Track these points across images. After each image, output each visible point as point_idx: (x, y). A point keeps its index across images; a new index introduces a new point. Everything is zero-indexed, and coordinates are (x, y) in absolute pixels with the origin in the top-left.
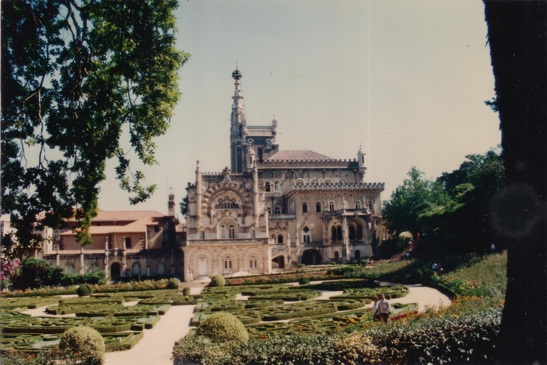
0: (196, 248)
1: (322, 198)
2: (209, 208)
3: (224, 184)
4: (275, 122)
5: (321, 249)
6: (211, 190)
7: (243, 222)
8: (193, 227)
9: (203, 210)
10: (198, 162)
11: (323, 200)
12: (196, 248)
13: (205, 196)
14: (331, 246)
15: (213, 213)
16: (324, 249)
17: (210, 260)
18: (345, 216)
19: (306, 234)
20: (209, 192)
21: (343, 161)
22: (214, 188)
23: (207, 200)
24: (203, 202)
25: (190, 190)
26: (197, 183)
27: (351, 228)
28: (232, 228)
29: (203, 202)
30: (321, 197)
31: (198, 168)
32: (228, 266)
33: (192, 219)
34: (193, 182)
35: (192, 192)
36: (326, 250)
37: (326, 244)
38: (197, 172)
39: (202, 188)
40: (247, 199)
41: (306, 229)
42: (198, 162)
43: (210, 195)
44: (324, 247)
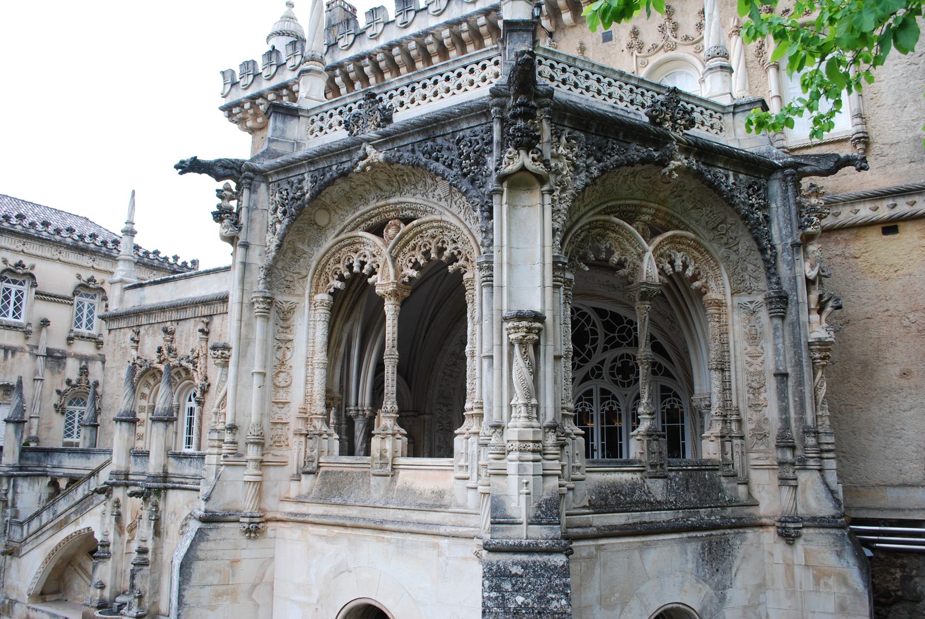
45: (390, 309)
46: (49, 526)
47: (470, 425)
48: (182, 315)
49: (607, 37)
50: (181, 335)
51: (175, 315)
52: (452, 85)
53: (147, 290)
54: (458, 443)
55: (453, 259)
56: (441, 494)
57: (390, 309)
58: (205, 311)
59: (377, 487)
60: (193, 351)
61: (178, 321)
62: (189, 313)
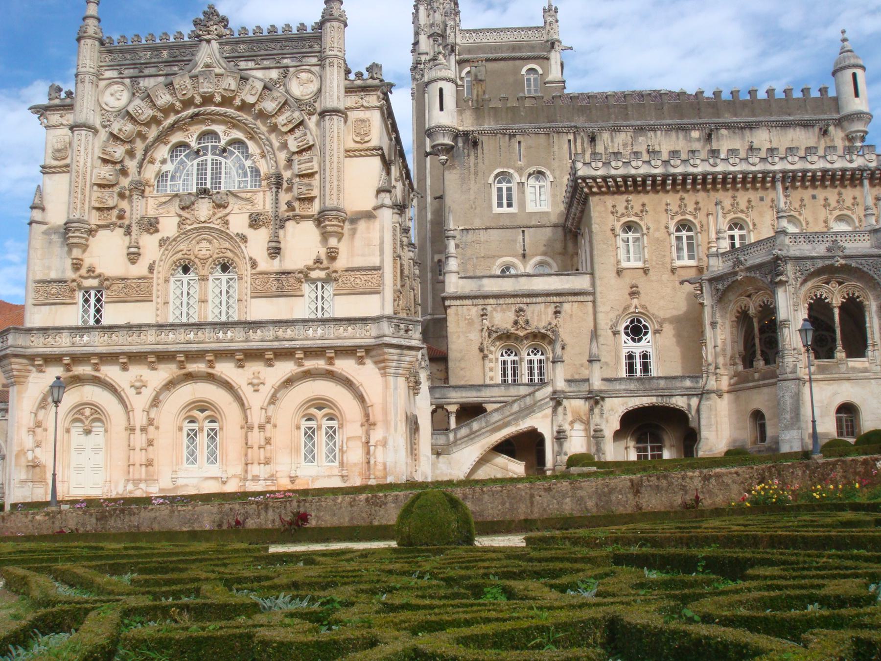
1: (697, 209)
4: (550, 11)
5: (694, 401)
7: (275, 251)
8: (53, 275)
14: (728, 392)
16: (705, 404)
18: (786, 259)
19: (637, 349)
21: (779, 94)
22: (148, 97)
23: (119, 151)
25: (54, 118)
27: (818, 312)
36: (710, 409)
37: (712, 384)
41: (636, 331)
43: (129, 127)
44: (703, 394)
45: (836, 311)
46: (484, 430)
47: (870, 348)
48: (534, 300)
49: (814, 197)
50: (533, 313)
51: (525, 300)
52: (853, 239)
53: (485, 281)
54: (870, 353)
55: (858, 297)
56: (866, 368)
57: (836, 311)
58: (555, 299)
59: (843, 368)
60: (550, 324)
61: (527, 304)
62: (539, 299)
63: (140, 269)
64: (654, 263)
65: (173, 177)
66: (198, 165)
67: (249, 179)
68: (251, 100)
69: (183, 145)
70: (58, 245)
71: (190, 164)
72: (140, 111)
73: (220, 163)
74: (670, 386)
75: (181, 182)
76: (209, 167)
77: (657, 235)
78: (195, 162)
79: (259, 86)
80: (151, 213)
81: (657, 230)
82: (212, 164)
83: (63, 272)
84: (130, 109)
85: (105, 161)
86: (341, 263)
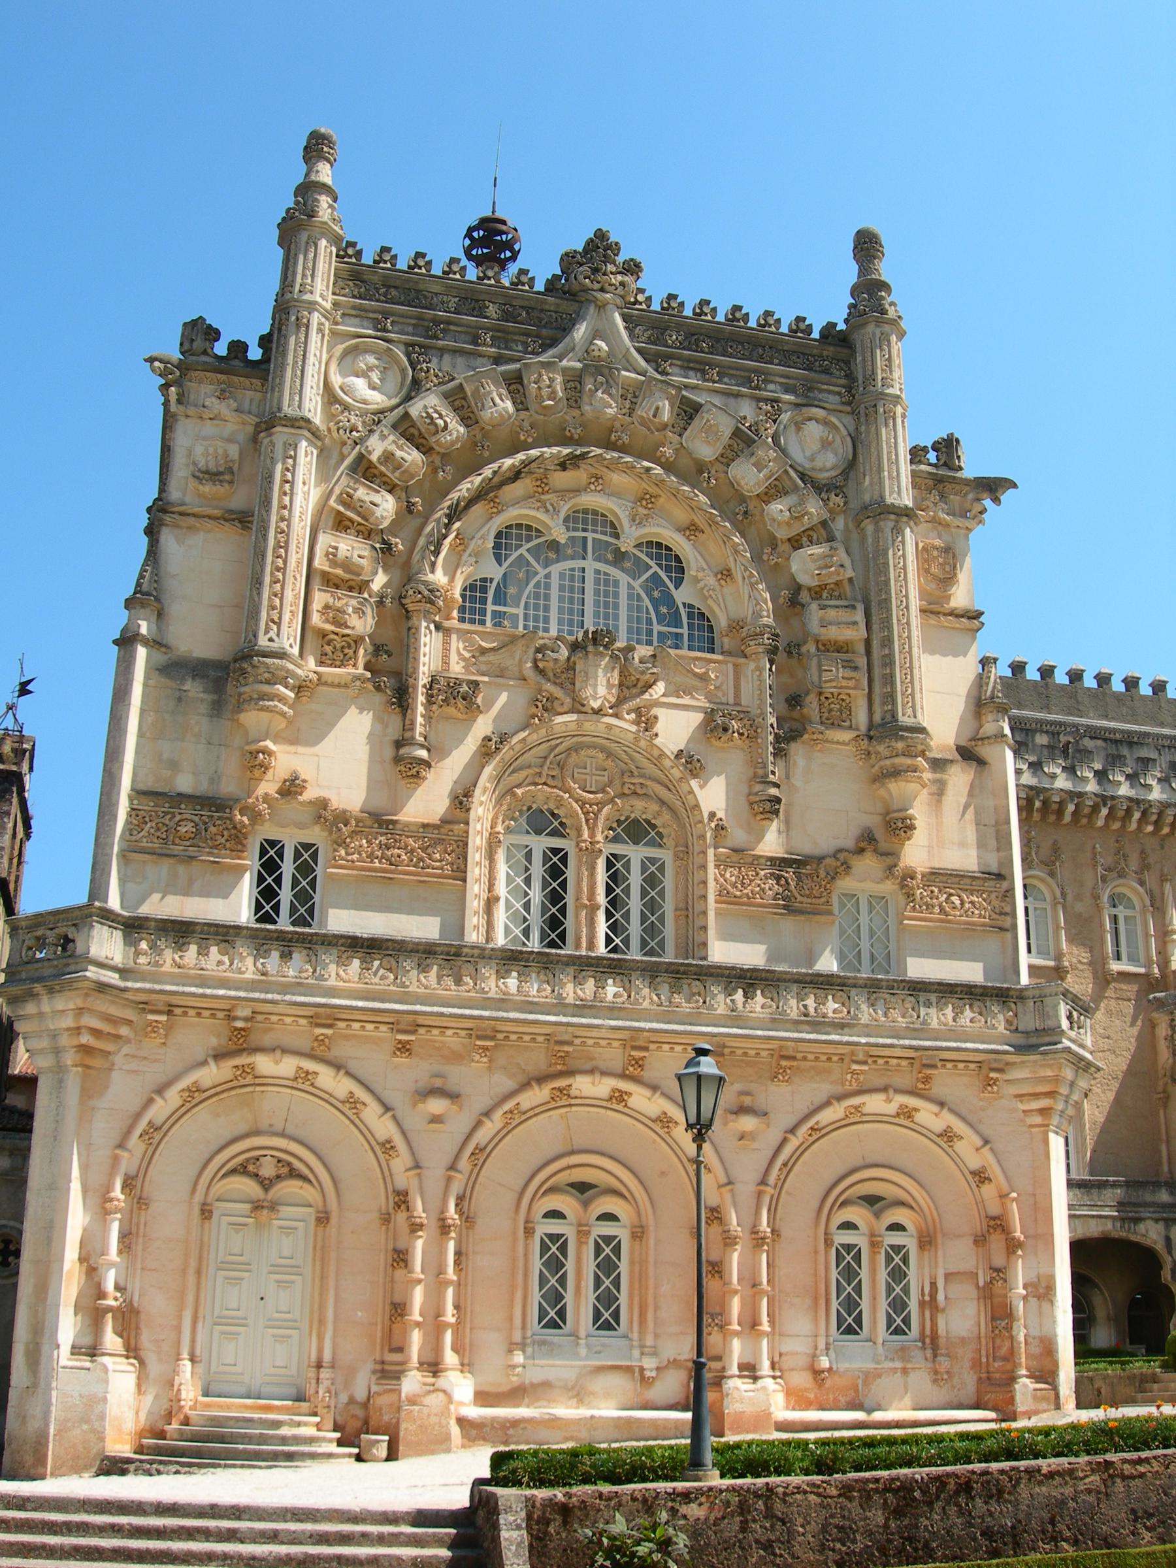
0: (196, 1036)
1: (1145, 866)
2: (404, 608)
3: (574, 382)
6: (429, 403)
8: (184, 783)
9: (320, 598)
10: (317, 147)
11: (1150, 878)
12: (196, 1036)
13: (364, 470)
15: (434, 653)
17: (364, 1200)
20: (407, 430)
22: (459, 401)
24: (344, 519)
26: (287, 311)
28: (635, 853)
29: (344, 519)
30: (1134, 865)
31: (308, 189)
32: (581, 1305)
33: (193, 688)
34: (244, 323)
35: (224, 409)
38: (295, 229)
39: (335, 375)
40: (805, 565)
42: (317, 147)
43: (411, 456)
63: (426, 803)
64: (1074, 960)
65: (500, 598)
66: (562, 576)
67: (685, 631)
68: (706, 451)
69: (526, 530)
70: (203, 708)
71: (542, 572)
72: (440, 422)
73: (616, 583)
74: (1133, 1200)
75: (520, 611)
76: (589, 586)
77: (1079, 907)
78: (556, 569)
79: (726, 427)
80: (456, 668)
81: (1079, 897)
82: (597, 582)
83: (215, 778)
84: (416, 409)
85: (341, 524)
86: (917, 854)
